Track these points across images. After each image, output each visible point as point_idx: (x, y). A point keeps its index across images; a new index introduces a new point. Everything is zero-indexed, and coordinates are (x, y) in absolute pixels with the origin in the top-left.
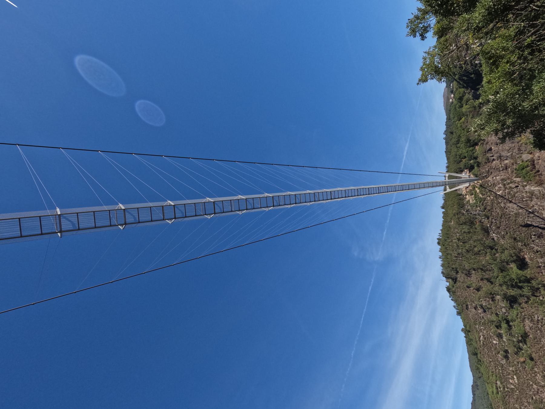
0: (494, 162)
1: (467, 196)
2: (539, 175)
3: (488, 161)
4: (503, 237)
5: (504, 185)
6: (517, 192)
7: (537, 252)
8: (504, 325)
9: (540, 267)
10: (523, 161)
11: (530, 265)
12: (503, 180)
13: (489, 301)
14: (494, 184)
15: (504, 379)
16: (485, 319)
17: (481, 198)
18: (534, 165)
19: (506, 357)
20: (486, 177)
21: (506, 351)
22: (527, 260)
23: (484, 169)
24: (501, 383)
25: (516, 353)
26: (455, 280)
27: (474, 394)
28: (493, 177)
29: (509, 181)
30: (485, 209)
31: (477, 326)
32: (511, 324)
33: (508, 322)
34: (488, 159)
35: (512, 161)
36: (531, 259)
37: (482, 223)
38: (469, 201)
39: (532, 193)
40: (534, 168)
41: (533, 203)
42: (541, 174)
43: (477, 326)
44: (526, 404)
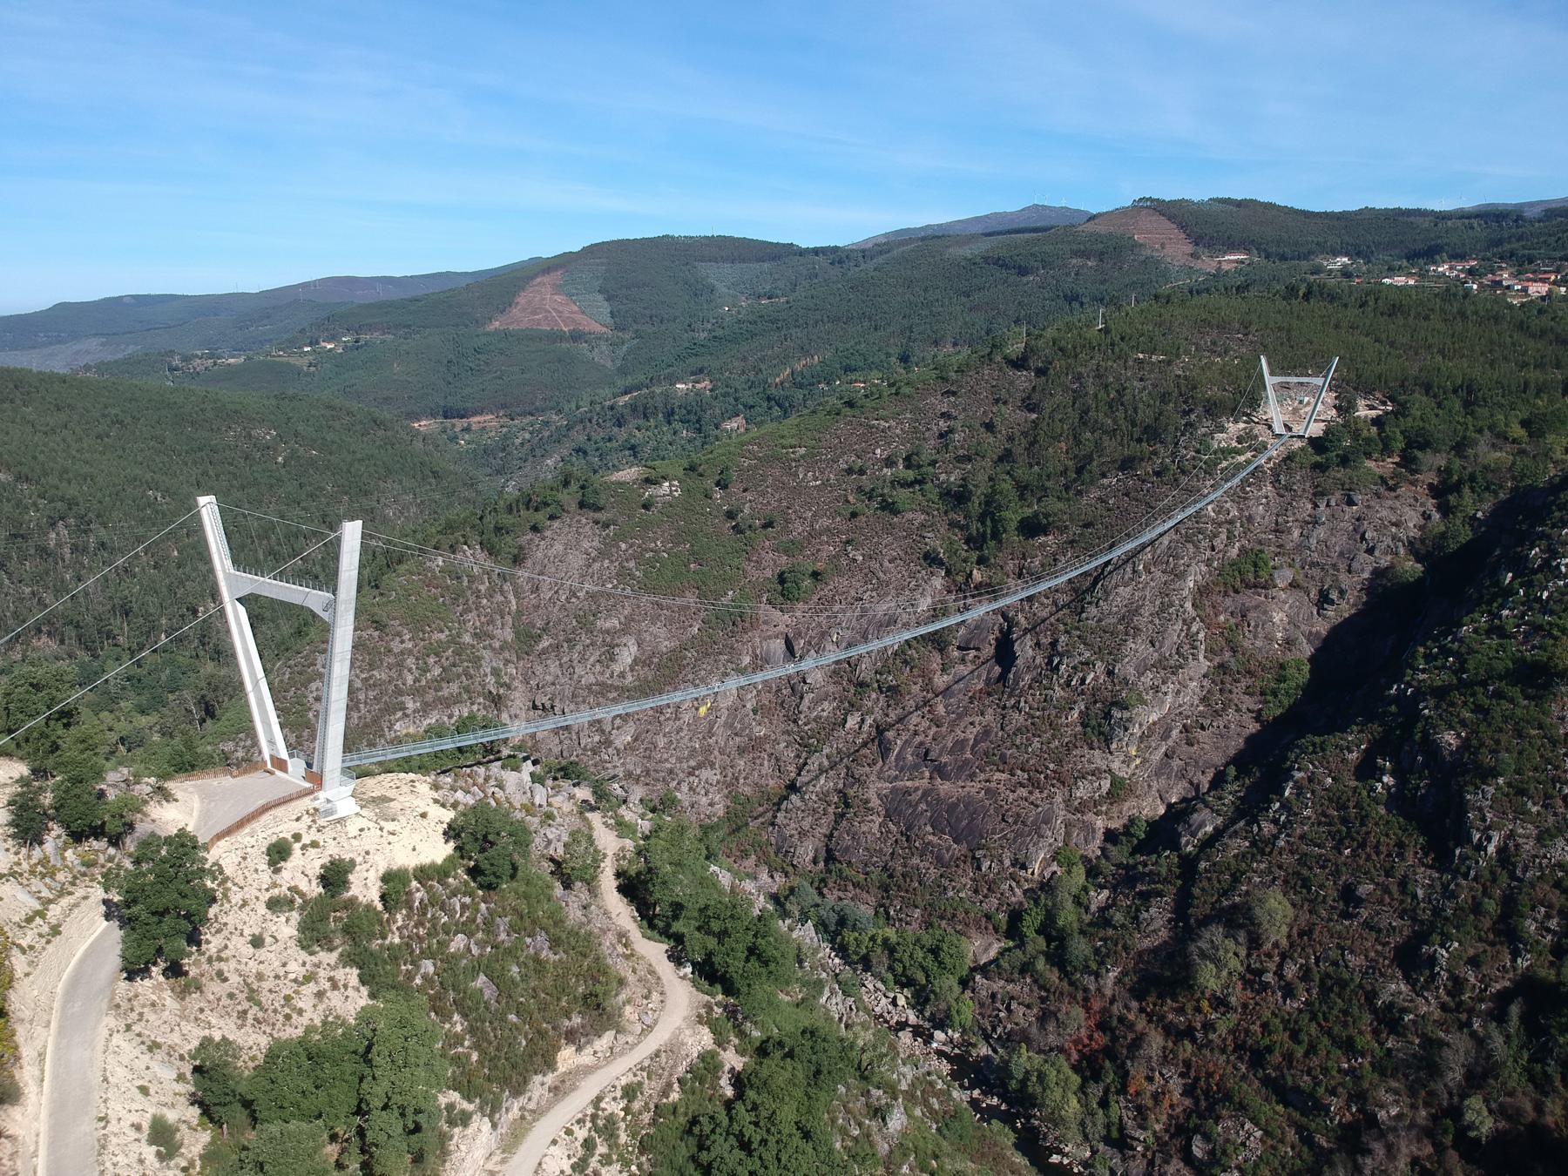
0: (1309, 506)
1: (1242, 425)
2: (1226, 592)
3: (1319, 493)
4: (1101, 500)
5: (1231, 522)
6: (1198, 548)
7: (1055, 560)
8: (911, 475)
9: (1024, 558)
10: (1274, 568)
11: (1031, 541)
12: (1250, 519)
13: (962, 447)
14: (1245, 499)
15: (811, 459)
16: (927, 435)
17: (1216, 465)
18: (1255, 587)
19: (850, 471)
20: (1276, 481)
21: (862, 472)
22: (1043, 539)
23: (1300, 480)
24: (802, 457)
25: (860, 490)
26: (1019, 363)
27: (816, 251)
28: (1267, 497)
29: (1236, 533)
30: (1183, 472)
31: (908, 416)
32: (917, 487)
33: (921, 482)
34: (1323, 494)
35: (1289, 546)
36: (1043, 546)
37: (1150, 458)
38: (1222, 430)
39: (1181, 576)
40: (1248, 586)
41: (1160, 573)
42: (1226, 594)
43: (908, 416)
44: (777, 496)
